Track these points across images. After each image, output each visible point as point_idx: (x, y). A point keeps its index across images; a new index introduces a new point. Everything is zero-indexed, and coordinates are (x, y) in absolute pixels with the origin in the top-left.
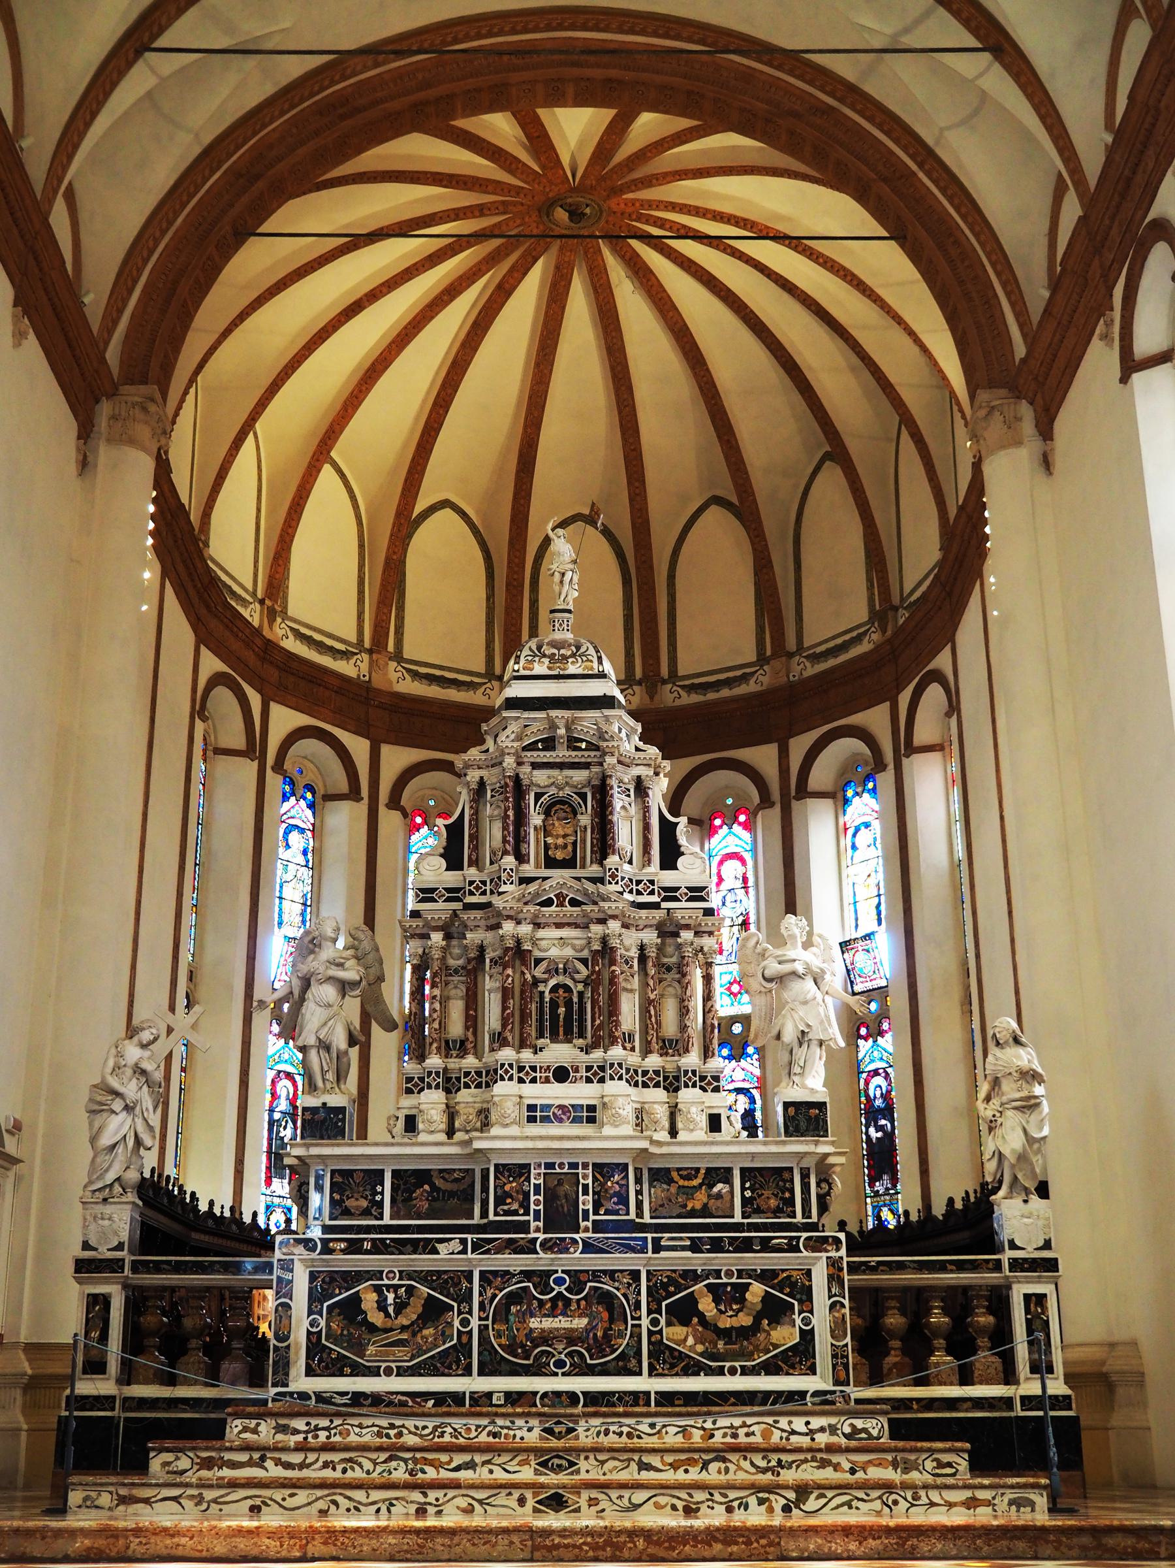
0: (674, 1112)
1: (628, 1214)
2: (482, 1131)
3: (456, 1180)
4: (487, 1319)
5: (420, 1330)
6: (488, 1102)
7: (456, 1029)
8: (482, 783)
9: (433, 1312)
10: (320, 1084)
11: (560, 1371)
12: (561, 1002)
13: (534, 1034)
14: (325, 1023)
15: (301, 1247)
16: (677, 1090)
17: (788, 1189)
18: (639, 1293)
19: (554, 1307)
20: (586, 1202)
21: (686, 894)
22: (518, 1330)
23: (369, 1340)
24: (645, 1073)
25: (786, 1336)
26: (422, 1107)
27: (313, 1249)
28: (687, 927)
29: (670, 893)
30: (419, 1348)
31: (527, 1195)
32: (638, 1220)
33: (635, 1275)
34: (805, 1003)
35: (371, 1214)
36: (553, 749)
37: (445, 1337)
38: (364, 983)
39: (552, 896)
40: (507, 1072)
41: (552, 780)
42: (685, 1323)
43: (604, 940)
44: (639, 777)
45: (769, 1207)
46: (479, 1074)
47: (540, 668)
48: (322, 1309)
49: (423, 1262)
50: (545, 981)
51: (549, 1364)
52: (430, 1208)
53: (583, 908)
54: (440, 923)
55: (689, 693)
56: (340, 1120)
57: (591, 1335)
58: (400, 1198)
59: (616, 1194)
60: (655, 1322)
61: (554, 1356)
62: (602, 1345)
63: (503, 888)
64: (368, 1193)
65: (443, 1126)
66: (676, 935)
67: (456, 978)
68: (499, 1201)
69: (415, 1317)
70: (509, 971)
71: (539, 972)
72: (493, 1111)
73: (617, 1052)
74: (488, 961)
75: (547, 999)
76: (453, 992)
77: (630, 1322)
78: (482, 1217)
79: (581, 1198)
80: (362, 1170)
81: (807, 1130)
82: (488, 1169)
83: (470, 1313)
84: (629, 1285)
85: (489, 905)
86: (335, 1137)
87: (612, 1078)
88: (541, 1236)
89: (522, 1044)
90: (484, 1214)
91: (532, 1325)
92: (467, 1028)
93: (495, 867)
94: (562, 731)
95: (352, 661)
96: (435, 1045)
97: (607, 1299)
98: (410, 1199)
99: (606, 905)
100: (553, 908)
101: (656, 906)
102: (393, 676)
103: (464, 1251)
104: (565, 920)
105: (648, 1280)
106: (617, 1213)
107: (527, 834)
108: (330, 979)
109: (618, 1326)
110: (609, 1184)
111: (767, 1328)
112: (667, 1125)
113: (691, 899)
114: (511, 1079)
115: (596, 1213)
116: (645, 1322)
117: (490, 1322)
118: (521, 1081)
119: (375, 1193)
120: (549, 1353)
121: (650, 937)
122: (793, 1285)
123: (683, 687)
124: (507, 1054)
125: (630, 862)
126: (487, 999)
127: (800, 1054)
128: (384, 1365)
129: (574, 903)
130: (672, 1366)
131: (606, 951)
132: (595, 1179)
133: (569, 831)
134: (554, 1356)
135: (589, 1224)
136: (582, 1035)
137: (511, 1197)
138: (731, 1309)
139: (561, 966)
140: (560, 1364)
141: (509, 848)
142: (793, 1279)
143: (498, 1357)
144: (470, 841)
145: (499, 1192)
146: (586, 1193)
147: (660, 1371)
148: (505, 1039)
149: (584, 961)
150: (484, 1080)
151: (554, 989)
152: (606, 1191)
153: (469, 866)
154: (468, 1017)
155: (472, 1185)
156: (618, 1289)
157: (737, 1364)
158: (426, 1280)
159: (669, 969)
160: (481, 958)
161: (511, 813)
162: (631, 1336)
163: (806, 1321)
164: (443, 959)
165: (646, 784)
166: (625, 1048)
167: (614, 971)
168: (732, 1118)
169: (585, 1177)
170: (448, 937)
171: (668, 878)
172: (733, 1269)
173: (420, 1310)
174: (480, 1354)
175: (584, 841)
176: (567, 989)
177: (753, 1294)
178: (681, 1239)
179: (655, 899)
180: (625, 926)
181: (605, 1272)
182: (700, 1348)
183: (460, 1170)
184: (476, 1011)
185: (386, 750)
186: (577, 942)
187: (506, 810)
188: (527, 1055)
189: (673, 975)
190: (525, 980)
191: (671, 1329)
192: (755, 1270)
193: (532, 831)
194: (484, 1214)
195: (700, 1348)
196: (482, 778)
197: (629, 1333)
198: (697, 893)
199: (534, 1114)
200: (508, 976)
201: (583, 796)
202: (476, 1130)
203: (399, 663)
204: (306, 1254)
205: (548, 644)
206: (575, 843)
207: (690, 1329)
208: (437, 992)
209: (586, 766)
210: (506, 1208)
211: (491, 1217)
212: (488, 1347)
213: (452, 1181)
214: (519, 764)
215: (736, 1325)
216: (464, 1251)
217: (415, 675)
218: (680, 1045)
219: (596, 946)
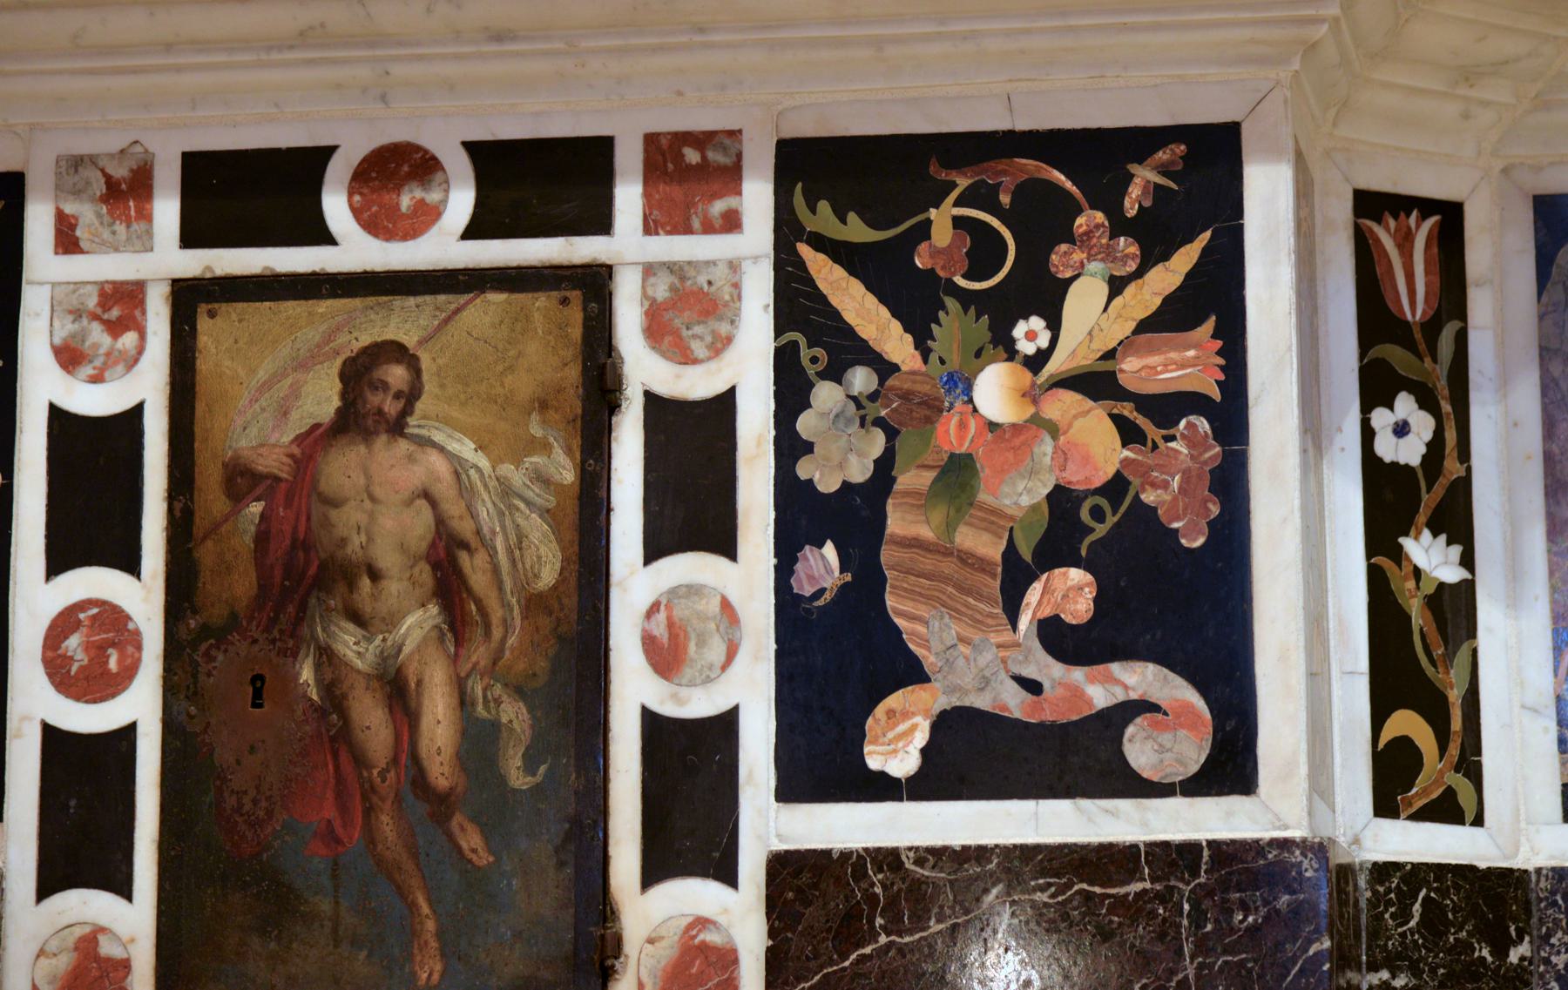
1: (1230, 767)
20: (699, 633)
59: (1062, 530)
79: (636, 584)
106: (1083, 758)
110: (995, 391)
115: (822, 763)
132: (811, 338)
135: (737, 913)
152: (957, 475)
169: (688, 313)
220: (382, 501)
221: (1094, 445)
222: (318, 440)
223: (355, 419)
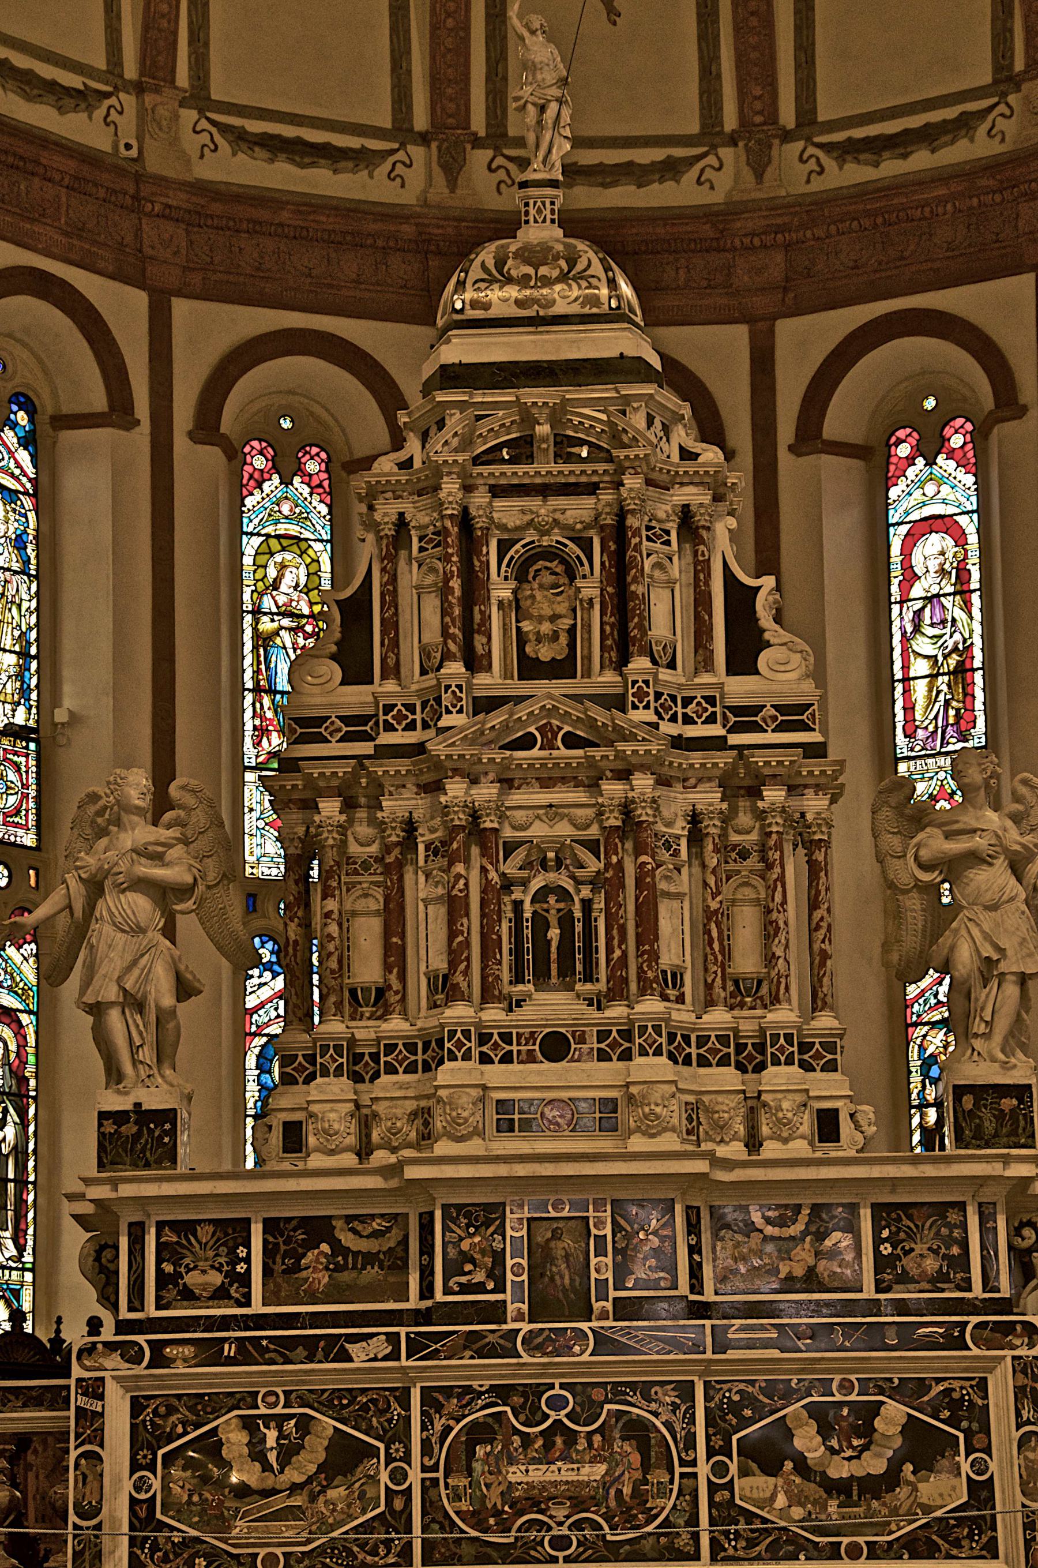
0: (754, 1106)
2: (417, 1146)
3: (376, 1234)
5: (323, 1491)
6: (428, 1097)
7: (367, 970)
8: (402, 523)
9: (344, 1459)
10: (128, 1068)
11: (561, 1555)
12: (553, 918)
13: (506, 976)
14: (135, 962)
15: (116, 1357)
16: (760, 1068)
17: (956, 1241)
18: (693, 1421)
19: (549, 1446)
21: (774, 718)
23: (237, 1510)
24: (702, 1041)
25: (943, 1491)
26: (314, 1108)
27: (137, 1360)
28: (775, 779)
29: (746, 717)
30: (322, 1520)
31: (499, 1258)
32: (693, 1297)
33: (686, 1391)
34: (993, 907)
35: (230, 1297)
36: (530, 459)
37: (365, 1501)
38: (201, 888)
39: (532, 729)
40: (459, 1045)
41: (529, 517)
42: (772, 1469)
43: (627, 809)
44: (686, 507)
45: (924, 1272)
46: (411, 1048)
47: (501, 298)
48: (154, 1460)
49: (323, 1374)
50: (525, 883)
51: (541, 1543)
52: (333, 1284)
53: (592, 748)
54: (335, 783)
55: (841, 161)
56: (166, 1133)
57: (612, 1492)
58: (279, 1268)
60: (720, 1469)
61: (550, 1529)
62: (632, 1509)
63: (446, 721)
64: (222, 1260)
65: (351, 1140)
66: (755, 793)
67: (366, 878)
68: (452, 1269)
69: (312, 1468)
70: (459, 868)
71: (511, 868)
72: (438, 1111)
73: (651, 1006)
74: (421, 847)
75: (528, 915)
76: (361, 905)
77: (678, 1470)
78: (422, 1297)
79: (593, 1261)
80: (210, 1221)
81: (996, 1135)
82: (431, 1214)
83: (407, 1459)
84: (675, 1407)
85: (420, 748)
86: (159, 1163)
87: (643, 1053)
88: (525, 1327)
89: (488, 995)
90: (426, 1291)
91: (512, 1478)
92: (387, 968)
93: (430, 680)
94: (543, 429)
95: (100, 113)
96: (333, 999)
97: (638, 1432)
98: (297, 1268)
99: (628, 748)
100: (535, 752)
101: (718, 744)
102: (191, 143)
103: (394, 1356)
104: (556, 774)
105: (707, 1398)
107: (486, 618)
108: (141, 884)
111: (911, 1478)
112: (741, 1129)
113: (781, 728)
114: (467, 1057)
116: (703, 1469)
117: (440, 1474)
118: (485, 1059)
119: (235, 1260)
120: (542, 1523)
121: (709, 798)
122: (955, 1405)
123: (828, 148)
124: (459, 1012)
125: (672, 665)
126: (422, 916)
127: (985, 996)
128: (262, 1552)
129: (572, 741)
130: (752, 1544)
131: (630, 825)
132: (616, 1227)
133: (562, 608)
135: (609, 1306)
136: (589, 977)
137: (473, 1261)
138: (851, 1446)
139: (551, 855)
141: (452, 647)
142: (956, 1395)
144: (383, 633)
145: (452, 1252)
146: (601, 1252)
147: (731, 1552)
148: (456, 987)
149: (592, 846)
150: (420, 1057)
151: (540, 896)
153: (384, 677)
154: (388, 948)
155: (405, 1242)
156: (656, 1414)
157: (861, 1540)
158: (329, 1405)
159: (744, 855)
160: (409, 842)
161: (455, 584)
163: (979, 1467)
164: (344, 843)
165: (701, 520)
166: (665, 998)
167: (644, 863)
168: (859, 1117)
169: (600, 1223)
170: (349, 805)
171: (740, 689)
172: (853, 1377)
173: (322, 1456)
175: (588, 627)
176: (564, 895)
177: (889, 1422)
178: (763, 1328)
179: (716, 730)
180: (664, 782)
182: (797, 1512)
183: (382, 1216)
184: (403, 936)
185: (181, 308)
186: (580, 812)
187: (447, 580)
188: (494, 1014)
189: (753, 862)
190: (488, 882)
191: (748, 1481)
192: (890, 1380)
193: (494, 609)
194: (426, 1291)
195: (797, 1512)
196: (401, 515)
198: (792, 715)
199: (509, 1118)
200: (459, 876)
201: (586, 546)
202: (409, 1146)
203: (201, 112)
204: (126, 1369)
205: (516, 255)
206: (572, 631)
207: (780, 1481)
208: (331, 905)
209: (592, 489)
210: (463, 1279)
211: (439, 1297)
213: (367, 1237)
214: (468, 489)
215: (860, 1473)
216: (394, 1356)
217: (240, 138)
218: (764, 990)
219: (614, 820)
220: (559, 1248)
221: (655, 1241)
222: (548, 1240)
223: (553, 1237)
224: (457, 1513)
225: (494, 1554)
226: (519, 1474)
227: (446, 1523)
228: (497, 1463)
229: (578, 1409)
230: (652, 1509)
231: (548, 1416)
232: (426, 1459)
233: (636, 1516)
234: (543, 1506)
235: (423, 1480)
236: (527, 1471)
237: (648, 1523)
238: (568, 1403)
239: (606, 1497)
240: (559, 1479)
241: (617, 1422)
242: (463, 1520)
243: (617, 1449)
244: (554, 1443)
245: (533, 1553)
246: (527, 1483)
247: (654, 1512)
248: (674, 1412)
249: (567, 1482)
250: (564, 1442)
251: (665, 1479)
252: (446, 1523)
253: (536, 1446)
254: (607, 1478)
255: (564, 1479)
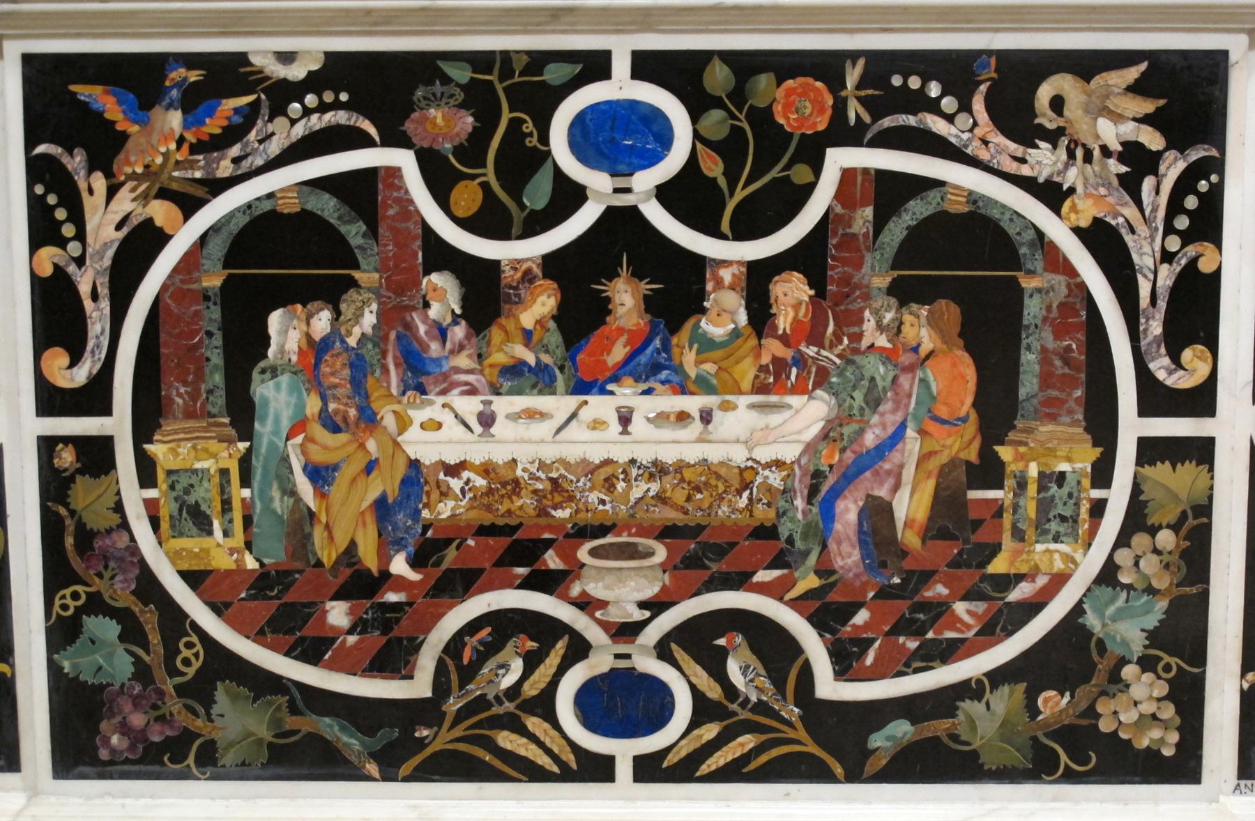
4: (94, 398)
11: (624, 751)
19: (581, 317)
22: (319, 475)
51: (544, 705)
57: (848, 511)
61: (579, 649)
77: (1133, 426)
84: (1139, 162)
91: (423, 446)
97: (966, 265)
109: (1050, 448)
117: (117, 424)
120: (545, 630)
134: (579, 649)
140: (624, 703)
143: (192, 659)
156: (1052, 195)
162: (1137, 519)
174: (62, 633)
181: (957, 70)
197: (1118, 498)
212: (121, 592)
224: (193, 578)
225: (351, 742)
226: (452, 429)
227: (149, 618)
228: (358, 384)
229: (713, 167)
230: (1007, 581)
231: (569, 196)
232: (57, 360)
233: (939, 610)
234: (552, 560)
235: (48, 445)
236: (487, 420)
237: (993, 631)
238: (665, 138)
239: (821, 532)
240: (621, 455)
241: (880, 223)
242: (218, 609)
243: (871, 334)
244: (601, 309)
245: (507, 740)
246: (487, 470)
247: (1020, 593)
248: (1131, 185)
249: (658, 470)
250: (651, 304)
251: (1077, 460)
252: (149, 618)
253: (527, 319)
254: (829, 457)
255: (645, 455)
